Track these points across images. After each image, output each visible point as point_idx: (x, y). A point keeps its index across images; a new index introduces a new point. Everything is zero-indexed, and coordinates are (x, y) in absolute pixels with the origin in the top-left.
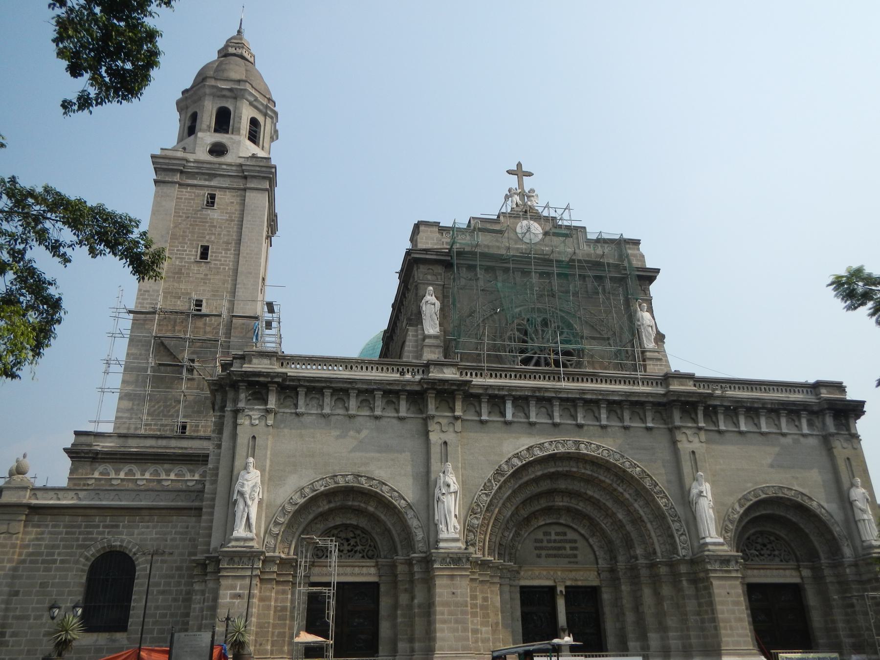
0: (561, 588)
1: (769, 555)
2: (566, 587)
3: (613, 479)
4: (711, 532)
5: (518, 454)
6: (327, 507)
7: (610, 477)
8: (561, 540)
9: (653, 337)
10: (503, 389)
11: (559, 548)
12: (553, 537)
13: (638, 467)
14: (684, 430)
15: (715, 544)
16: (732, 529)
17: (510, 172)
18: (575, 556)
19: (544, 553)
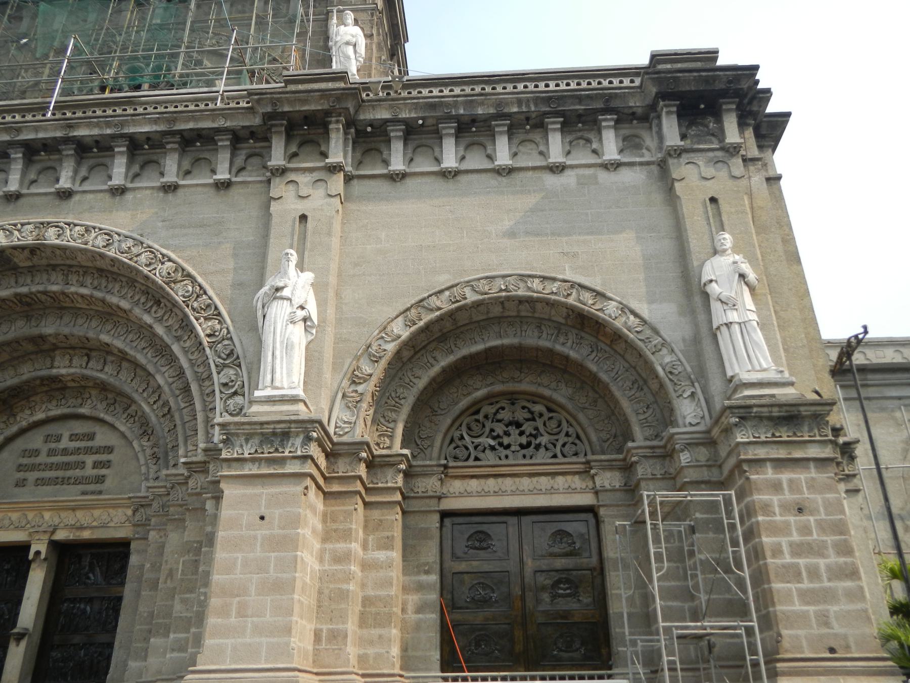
0: (40, 546)
1: (522, 447)
2: (55, 545)
3: (139, 300)
4: (278, 375)
8: (79, 449)
9: (358, 64)
11: (67, 466)
12: (65, 443)
13: (170, 260)
15: (270, 400)
16: (371, 375)
18: (100, 479)
19: (32, 476)
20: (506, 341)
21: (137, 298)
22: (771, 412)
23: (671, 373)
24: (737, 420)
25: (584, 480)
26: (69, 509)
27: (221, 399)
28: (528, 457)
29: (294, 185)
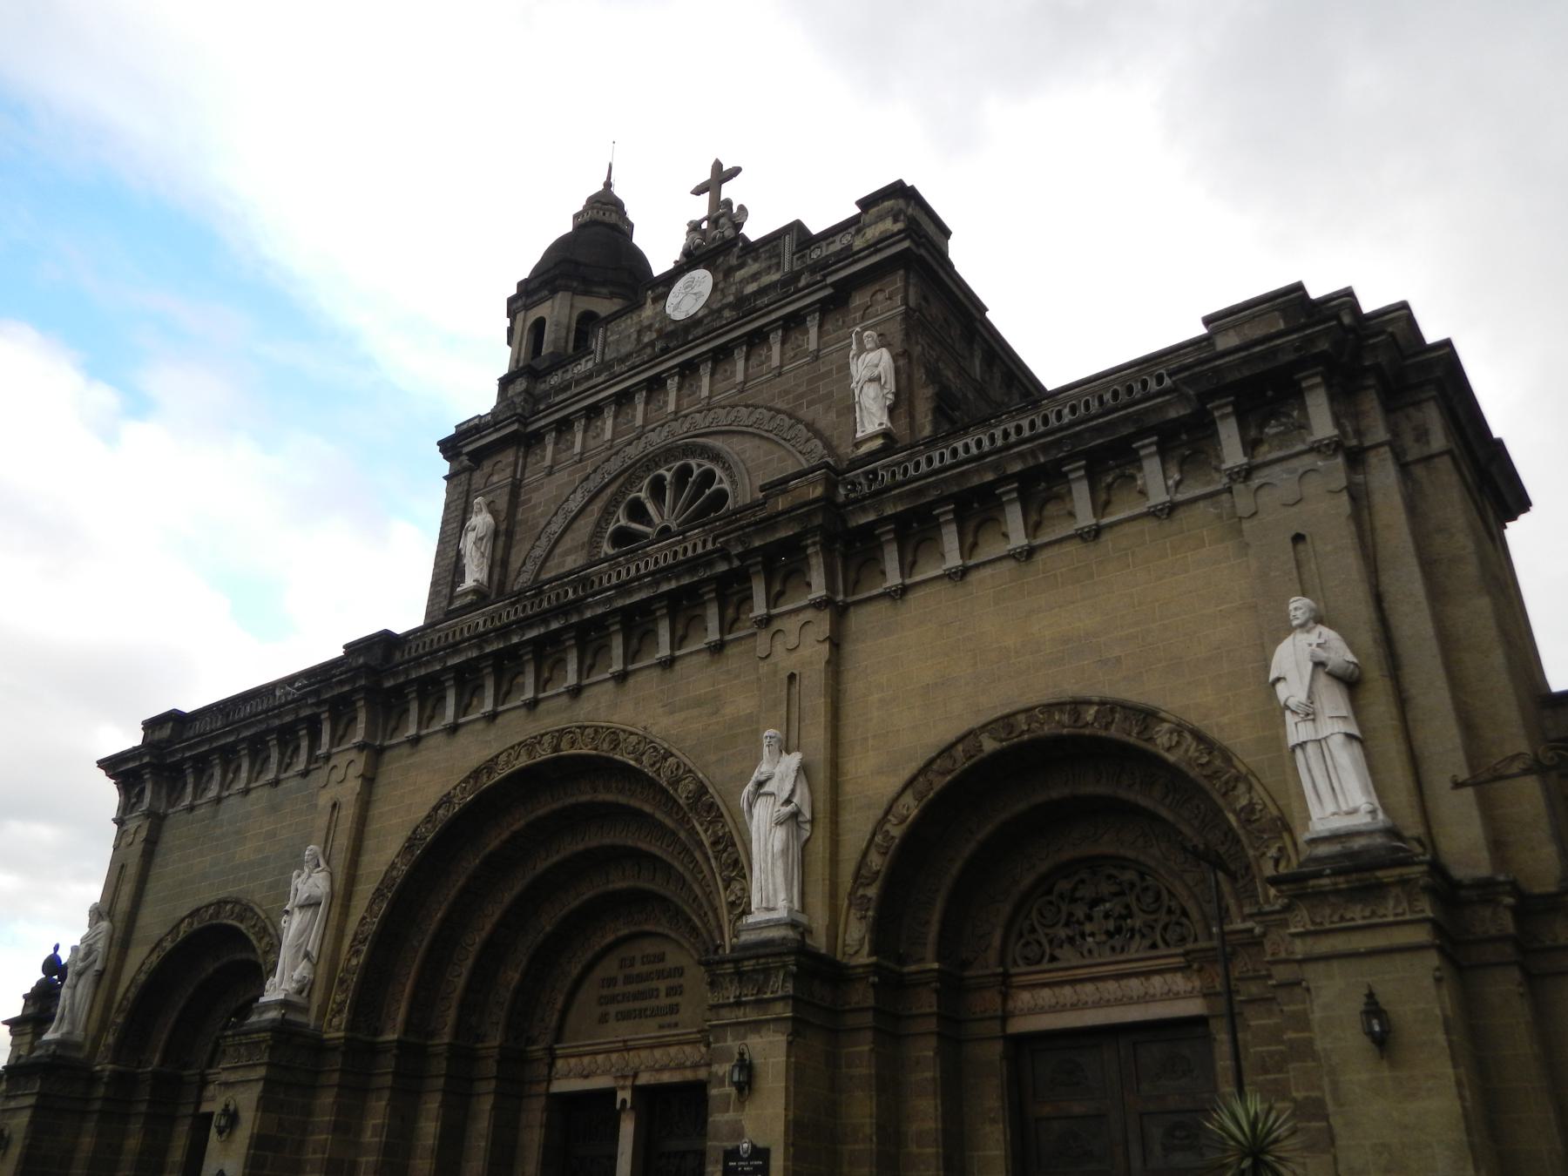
0: (624, 1095)
1: (1110, 934)
2: (638, 1091)
3: (660, 801)
5: (449, 793)
6: (211, 970)
7: (654, 798)
8: (651, 973)
9: (888, 403)
10: (428, 662)
12: (639, 968)
14: (776, 625)
16: (878, 872)
17: (698, 191)
19: (613, 1009)
20: (1055, 795)
21: (658, 798)
22: (1336, 884)
23: (1249, 821)
24: (1286, 901)
25: (1189, 979)
26: (647, 1048)
27: (730, 921)
28: (1118, 949)
29: (780, 634)
